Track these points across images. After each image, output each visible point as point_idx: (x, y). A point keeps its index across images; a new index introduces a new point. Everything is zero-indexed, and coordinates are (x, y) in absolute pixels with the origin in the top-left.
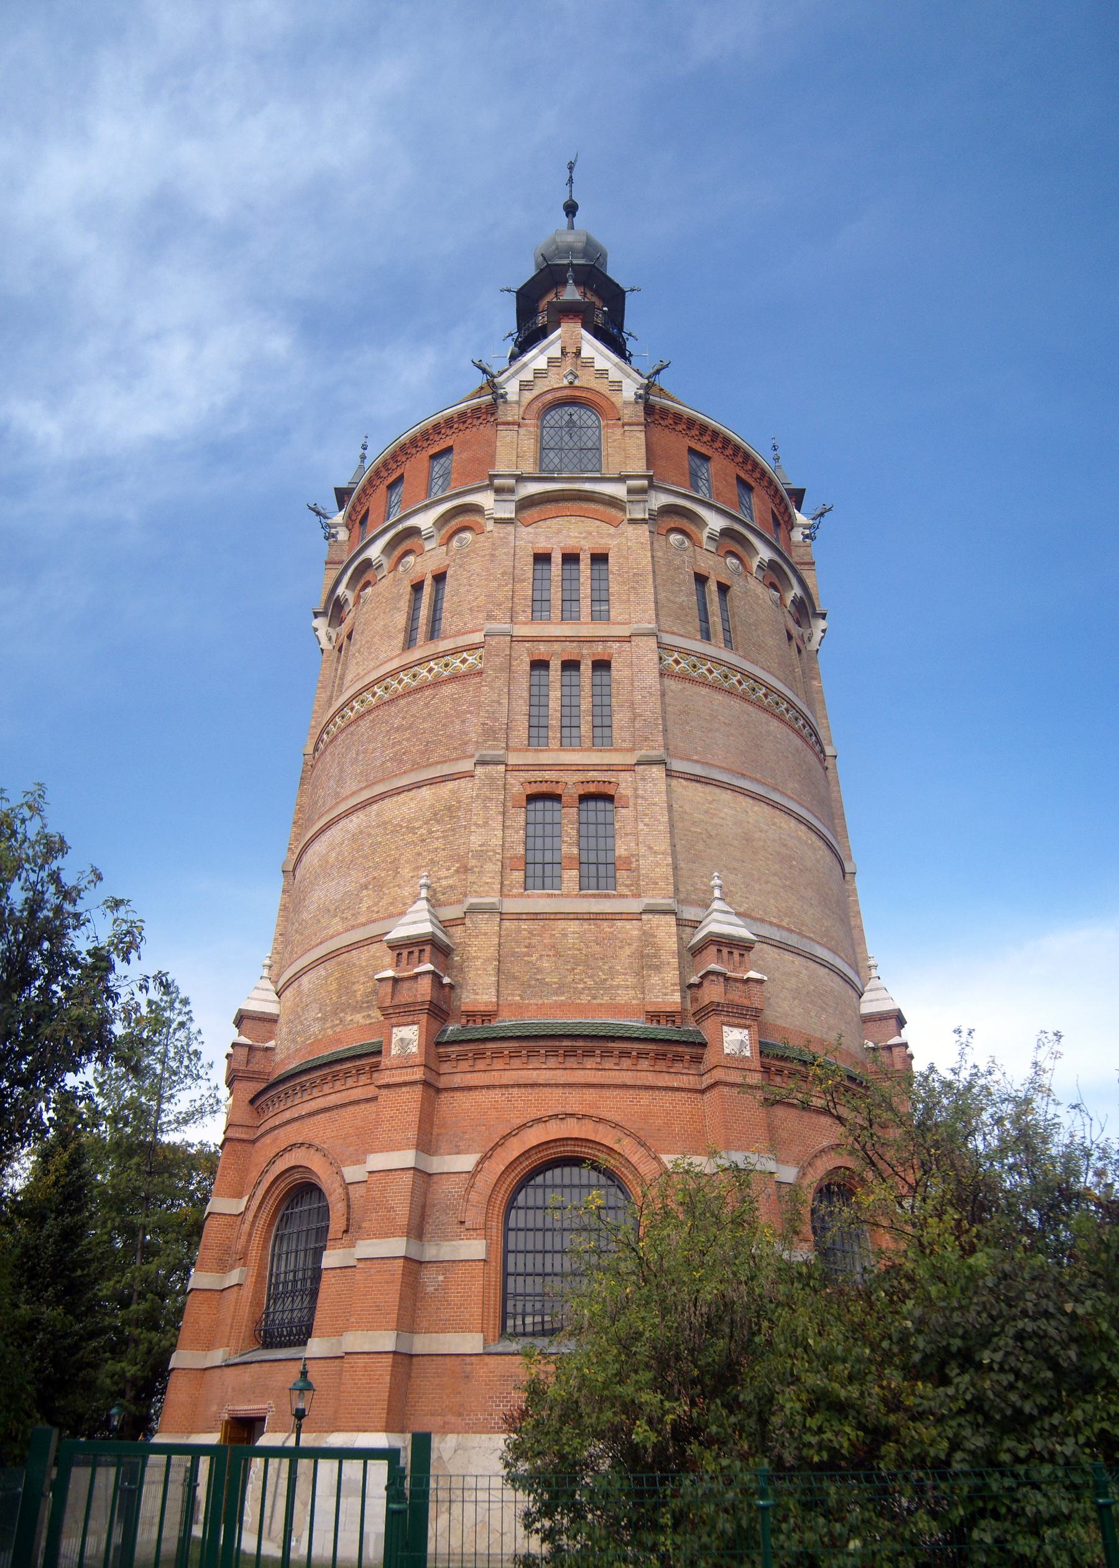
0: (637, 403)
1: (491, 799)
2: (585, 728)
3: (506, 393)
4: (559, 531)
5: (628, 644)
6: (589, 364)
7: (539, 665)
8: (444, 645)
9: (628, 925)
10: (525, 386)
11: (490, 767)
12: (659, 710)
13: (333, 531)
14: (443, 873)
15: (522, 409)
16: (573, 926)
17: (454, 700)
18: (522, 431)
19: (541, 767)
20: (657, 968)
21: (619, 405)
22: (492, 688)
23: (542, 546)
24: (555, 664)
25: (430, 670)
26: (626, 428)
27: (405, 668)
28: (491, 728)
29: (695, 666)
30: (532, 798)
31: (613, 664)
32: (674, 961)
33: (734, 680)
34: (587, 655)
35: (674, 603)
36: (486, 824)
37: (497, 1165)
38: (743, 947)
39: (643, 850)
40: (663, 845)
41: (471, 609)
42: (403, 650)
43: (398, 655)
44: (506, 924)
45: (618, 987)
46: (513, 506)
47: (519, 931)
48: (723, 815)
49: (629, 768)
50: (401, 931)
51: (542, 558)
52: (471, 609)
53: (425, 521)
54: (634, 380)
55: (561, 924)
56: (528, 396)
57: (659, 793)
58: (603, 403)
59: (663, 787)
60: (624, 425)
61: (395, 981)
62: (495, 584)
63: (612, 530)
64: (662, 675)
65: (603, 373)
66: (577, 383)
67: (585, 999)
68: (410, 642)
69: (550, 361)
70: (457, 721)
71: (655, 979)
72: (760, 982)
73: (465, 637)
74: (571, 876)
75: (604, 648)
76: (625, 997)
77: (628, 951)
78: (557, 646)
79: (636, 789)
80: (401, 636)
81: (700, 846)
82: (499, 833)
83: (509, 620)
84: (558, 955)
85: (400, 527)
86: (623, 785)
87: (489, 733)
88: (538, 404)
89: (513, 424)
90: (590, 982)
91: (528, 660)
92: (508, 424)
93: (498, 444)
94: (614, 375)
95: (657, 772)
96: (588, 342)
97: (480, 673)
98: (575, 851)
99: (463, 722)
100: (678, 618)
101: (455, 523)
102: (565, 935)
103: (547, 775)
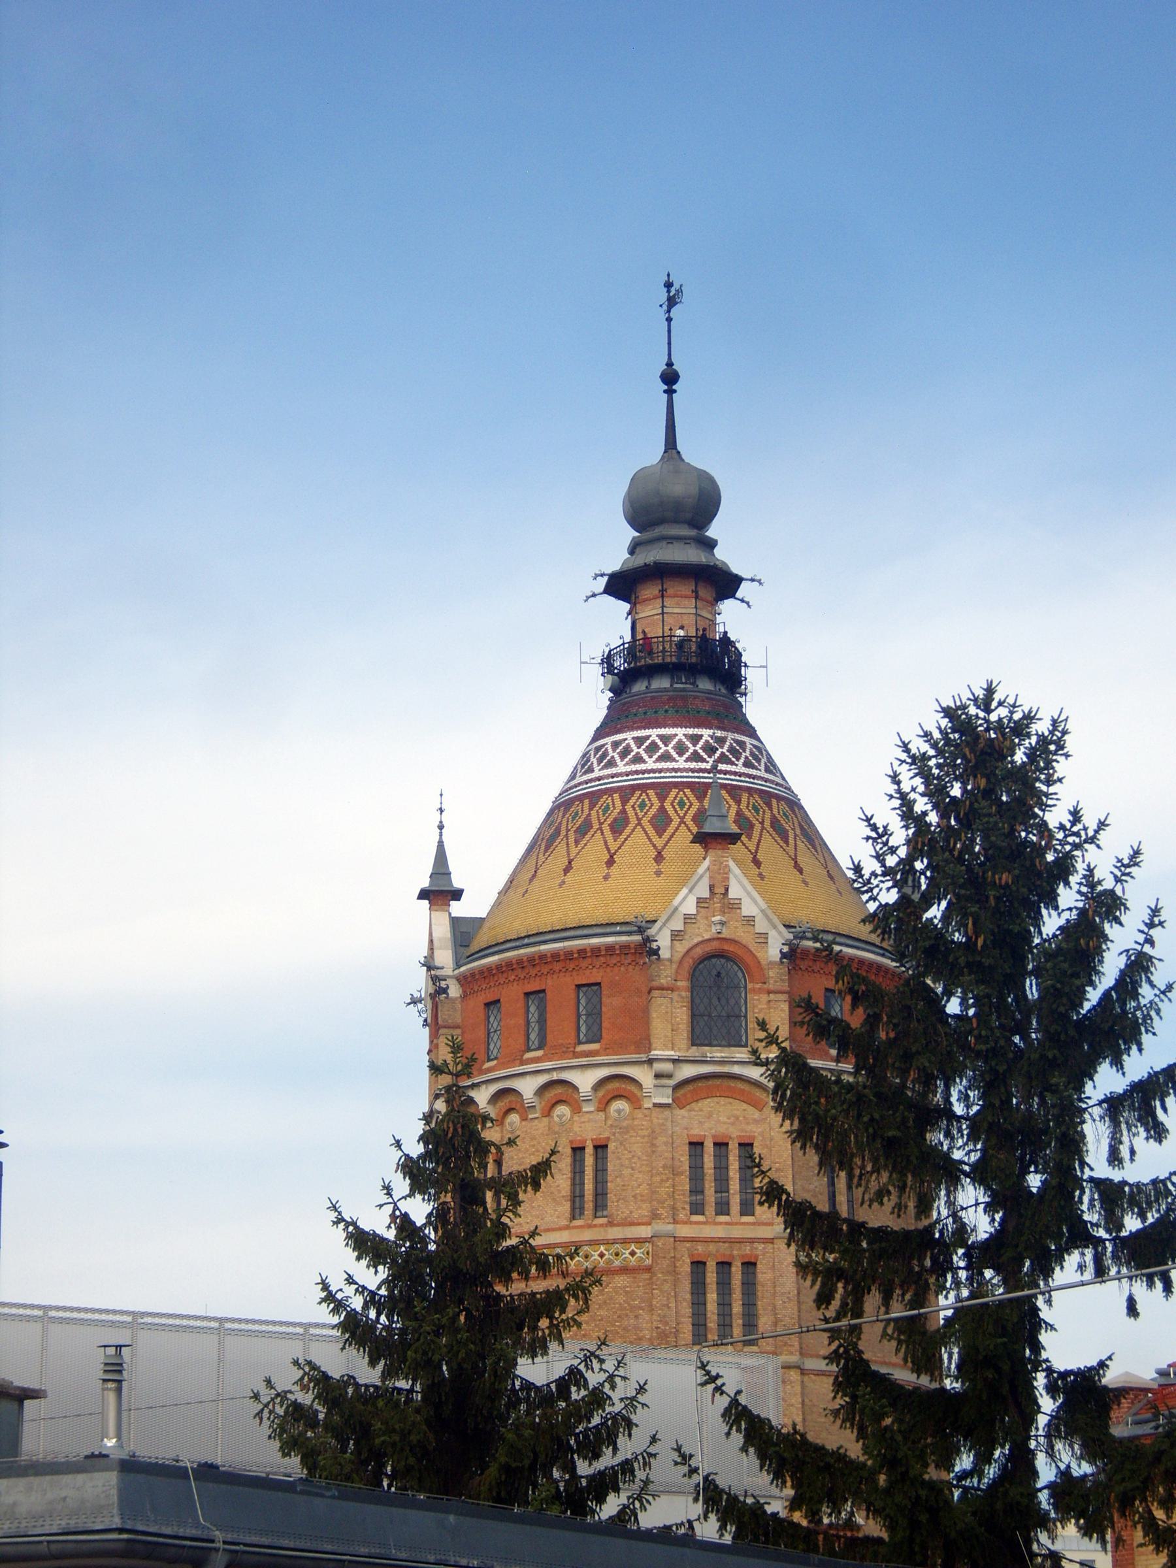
0: (782, 963)
2: (737, 1331)
3: (659, 948)
4: (710, 1116)
5: (771, 1246)
6: (735, 906)
7: (698, 1265)
8: (615, 1233)
10: (676, 936)
12: (795, 1316)
13: (443, 984)
15: (674, 966)
17: (627, 1292)
18: (675, 995)
21: (763, 962)
22: (661, 1291)
23: (697, 1132)
24: (711, 1266)
25: (602, 1255)
26: (772, 996)
28: (664, 1332)
31: (759, 1266)
34: (738, 1255)
35: (809, 1191)
41: (635, 1196)
46: (670, 1091)
51: (696, 1146)
52: (635, 1196)
53: (584, 1081)
54: (780, 933)
56: (682, 948)
57: (796, 1394)
58: (749, 960)
59: (798, 1389)
60: (769, 992)
62: (658, 1179)
63: (756, 1115)
65: (750, 921)
66: (726, 933)
69: (700, 901)
70: (631, 1315)
73: (633, 1228)
75: (751, 1250)
78: (712, 1247)
80: (567, 1206)
85: (555, 1076)
88: (688, 963)
89: (667, 989)
92: (662, 989)
93: (654, 1015)
94: (761, 926)
96: (736, 876)
97: (648, 1269)
99: (636, 1317)
101: (612, 1086)
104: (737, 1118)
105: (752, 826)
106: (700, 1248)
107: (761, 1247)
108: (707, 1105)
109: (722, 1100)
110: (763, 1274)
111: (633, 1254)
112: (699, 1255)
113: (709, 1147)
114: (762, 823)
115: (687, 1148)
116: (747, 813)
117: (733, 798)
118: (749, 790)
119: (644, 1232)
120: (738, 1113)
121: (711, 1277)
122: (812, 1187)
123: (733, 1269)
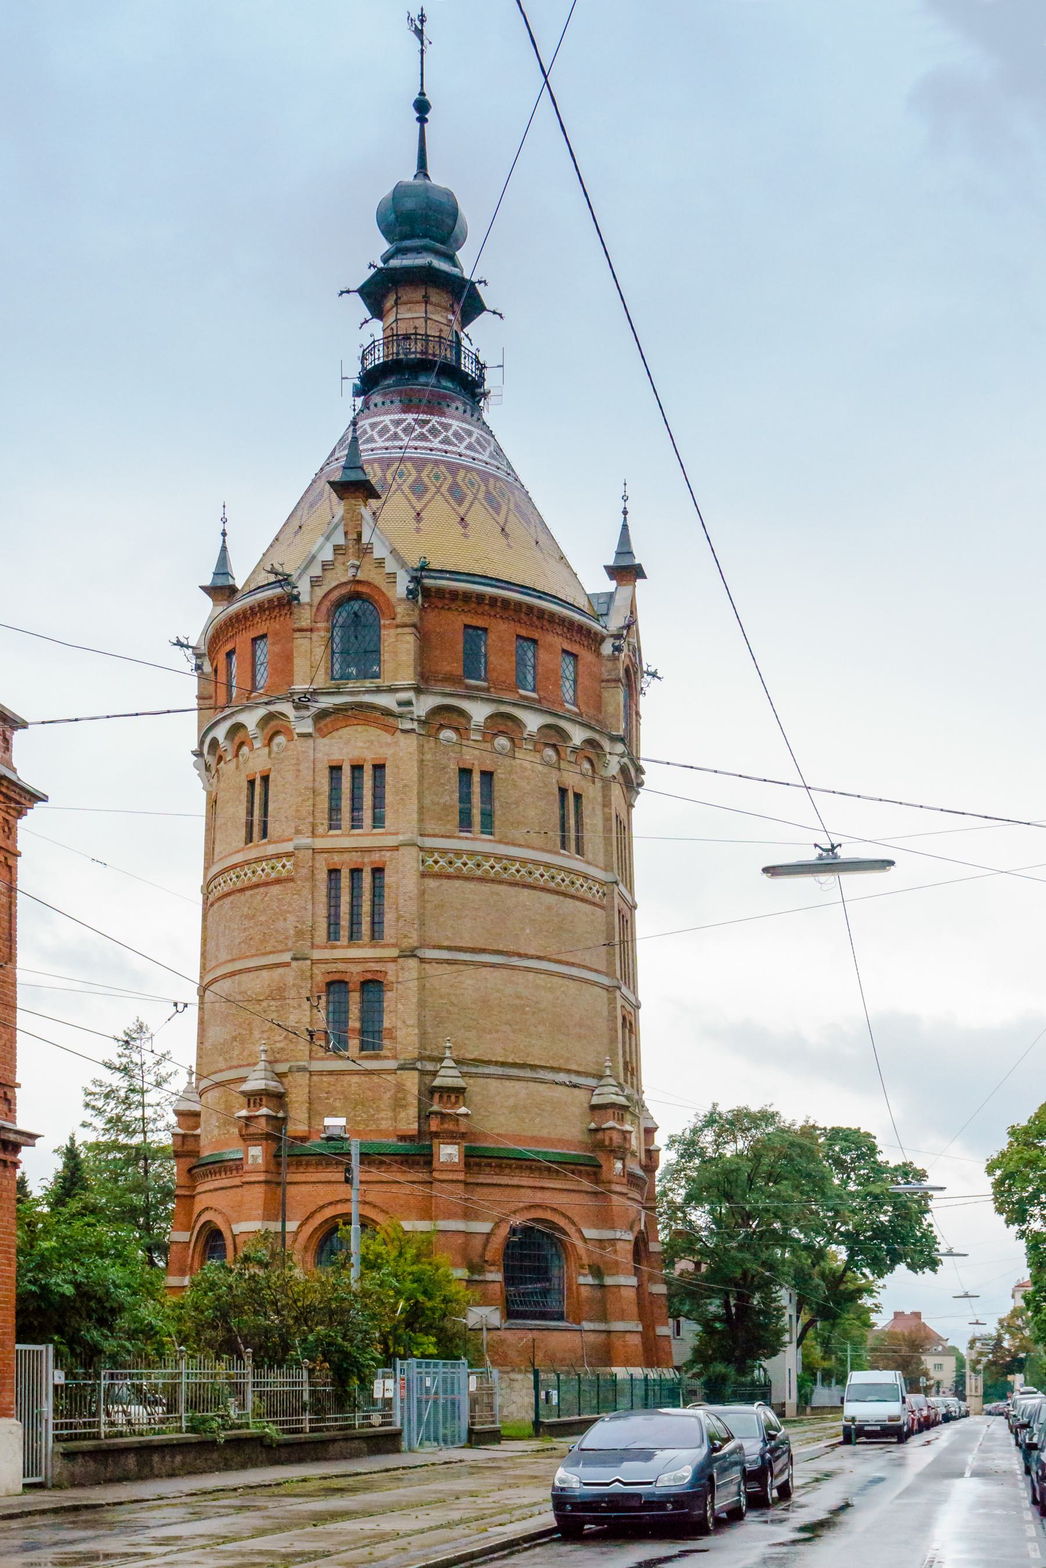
1: (302, 988)
8: (271, 849)
9: (389, 1078)
11: (300, 962)
14: (278, 1038)
16: (355, 1079)
17: (278, 899)
19: (335, 960)
20: (404, 1107)
23: (336, 757)
24: (345, 874)
27: (247, 863)
29: (450, 863)
30: (329, 984)
31: (386, 871)
32: (416, 1102)
33: (487, 866)
34: (368, 862)
35: (438, 804)
36: (300, 1006)
37: (309, 1229)
38: (460, 1091)
39: (399, 1024)
40: (412, 1021)
41: (286, 817)
42: (246, 844)
43: (243, 850)
44: (315, 1078)
45: (382, 1118)
47: (322, 1082)
48: (465, 986)
49: (394, 960)
50: (249, 1086)
55: (348, 1077)
61: (248, 1118)
64: (423, 875)
67: (361, 1127)
68: (249, 838)
71: (403, 1115)
72: (466, 1115)
74: (354, 1043)
75: (381, 856)
76: (385, 1125)
77: (389, 1094)
78: (346, 857)
79: (398, 977)
81: (444, 1014)
82: (308, 1013)
83: (310, 835)
84: (346, 1098)
86: (390, 973)
87: (299, 934)
90: (365, 1116)
91: (325, 870)
95: (412, 963)
98: (357, 1025)
99: (285, 919)
100: (440, 819)
102: (350, 1085)
103: (341, 967)
104: (372, 742)
105: (426, 489)
106: (336, 858)
107: (388, 854)
108: (345, 732)
109: (359, 728)
110: (389, 878)
111: (284, 866)
112: (335, 864)
113: (347, 771)
114: (438, 489)
115: (327, 772)
116: (426, 480)
117: (416, 468)
118: (436, 463)
119: (289, 847)
120: (373, 738)
121: (345, 881)
122: (442, 801)
123: (364, 874)
